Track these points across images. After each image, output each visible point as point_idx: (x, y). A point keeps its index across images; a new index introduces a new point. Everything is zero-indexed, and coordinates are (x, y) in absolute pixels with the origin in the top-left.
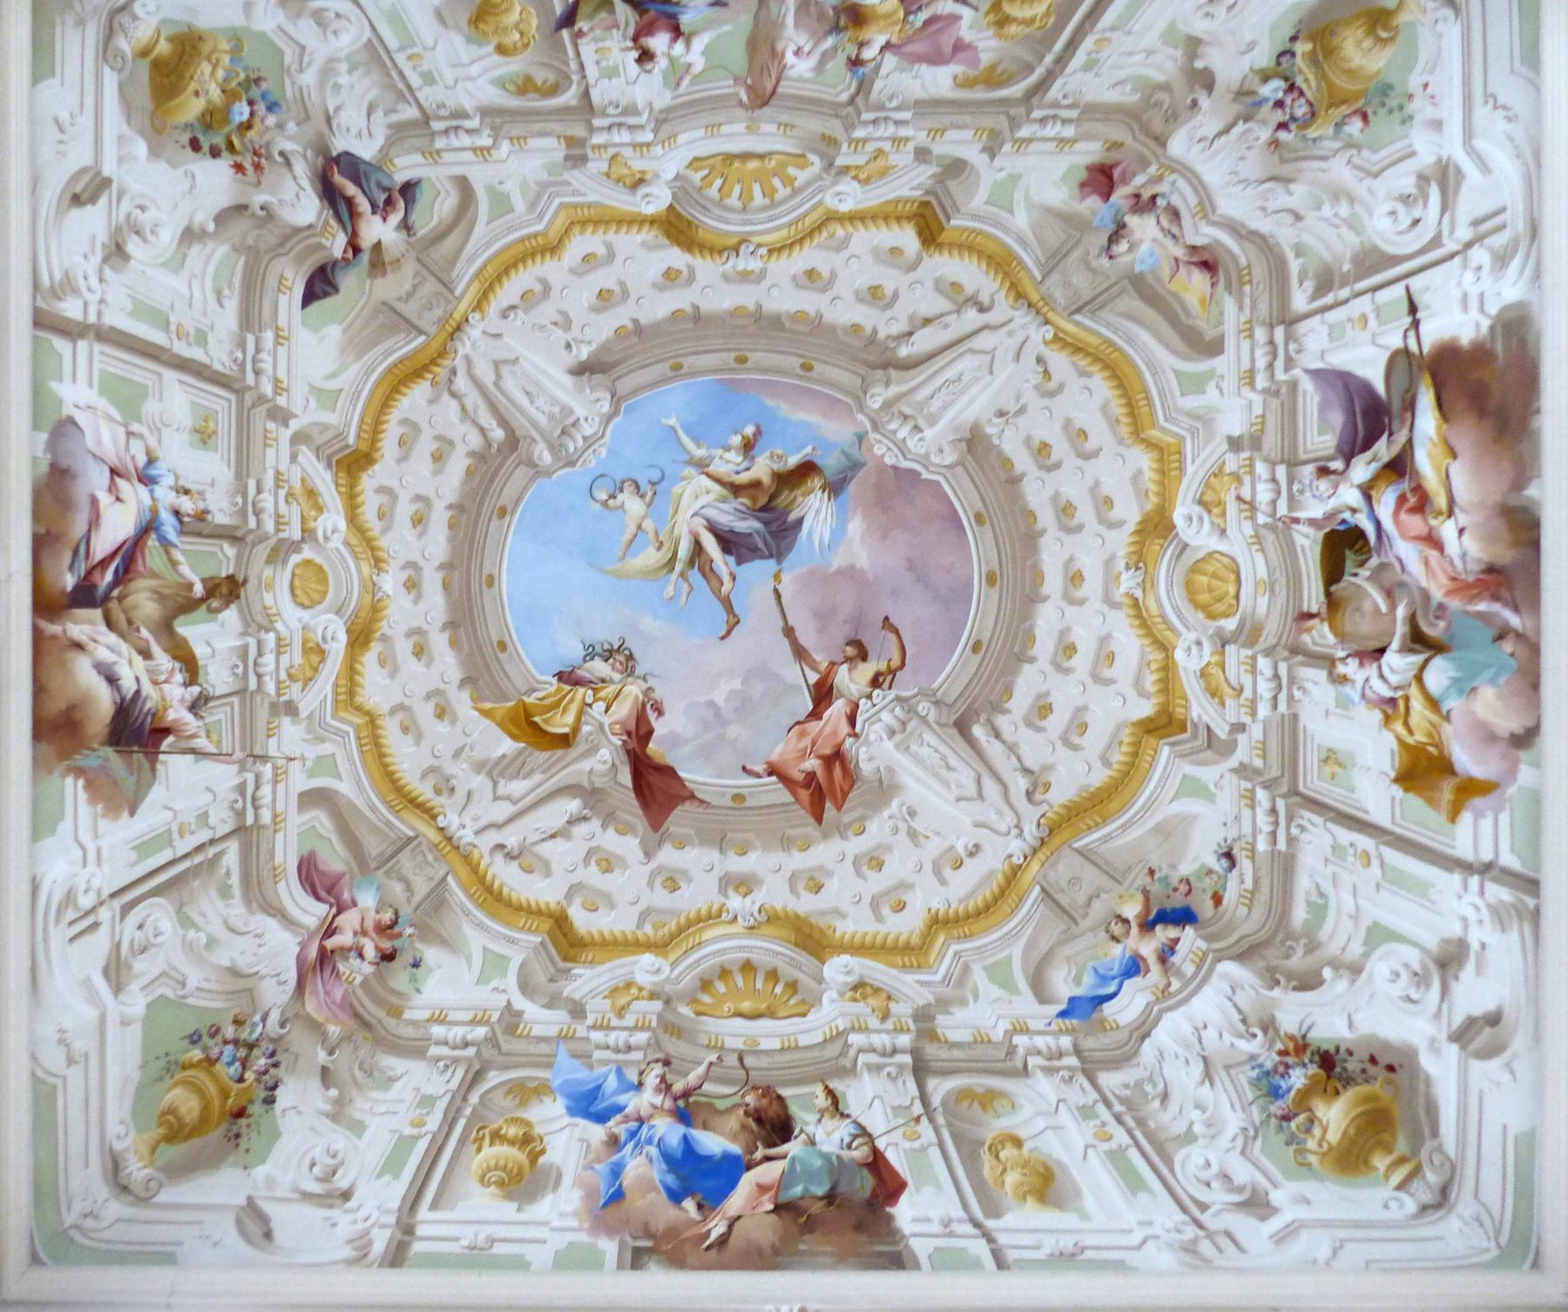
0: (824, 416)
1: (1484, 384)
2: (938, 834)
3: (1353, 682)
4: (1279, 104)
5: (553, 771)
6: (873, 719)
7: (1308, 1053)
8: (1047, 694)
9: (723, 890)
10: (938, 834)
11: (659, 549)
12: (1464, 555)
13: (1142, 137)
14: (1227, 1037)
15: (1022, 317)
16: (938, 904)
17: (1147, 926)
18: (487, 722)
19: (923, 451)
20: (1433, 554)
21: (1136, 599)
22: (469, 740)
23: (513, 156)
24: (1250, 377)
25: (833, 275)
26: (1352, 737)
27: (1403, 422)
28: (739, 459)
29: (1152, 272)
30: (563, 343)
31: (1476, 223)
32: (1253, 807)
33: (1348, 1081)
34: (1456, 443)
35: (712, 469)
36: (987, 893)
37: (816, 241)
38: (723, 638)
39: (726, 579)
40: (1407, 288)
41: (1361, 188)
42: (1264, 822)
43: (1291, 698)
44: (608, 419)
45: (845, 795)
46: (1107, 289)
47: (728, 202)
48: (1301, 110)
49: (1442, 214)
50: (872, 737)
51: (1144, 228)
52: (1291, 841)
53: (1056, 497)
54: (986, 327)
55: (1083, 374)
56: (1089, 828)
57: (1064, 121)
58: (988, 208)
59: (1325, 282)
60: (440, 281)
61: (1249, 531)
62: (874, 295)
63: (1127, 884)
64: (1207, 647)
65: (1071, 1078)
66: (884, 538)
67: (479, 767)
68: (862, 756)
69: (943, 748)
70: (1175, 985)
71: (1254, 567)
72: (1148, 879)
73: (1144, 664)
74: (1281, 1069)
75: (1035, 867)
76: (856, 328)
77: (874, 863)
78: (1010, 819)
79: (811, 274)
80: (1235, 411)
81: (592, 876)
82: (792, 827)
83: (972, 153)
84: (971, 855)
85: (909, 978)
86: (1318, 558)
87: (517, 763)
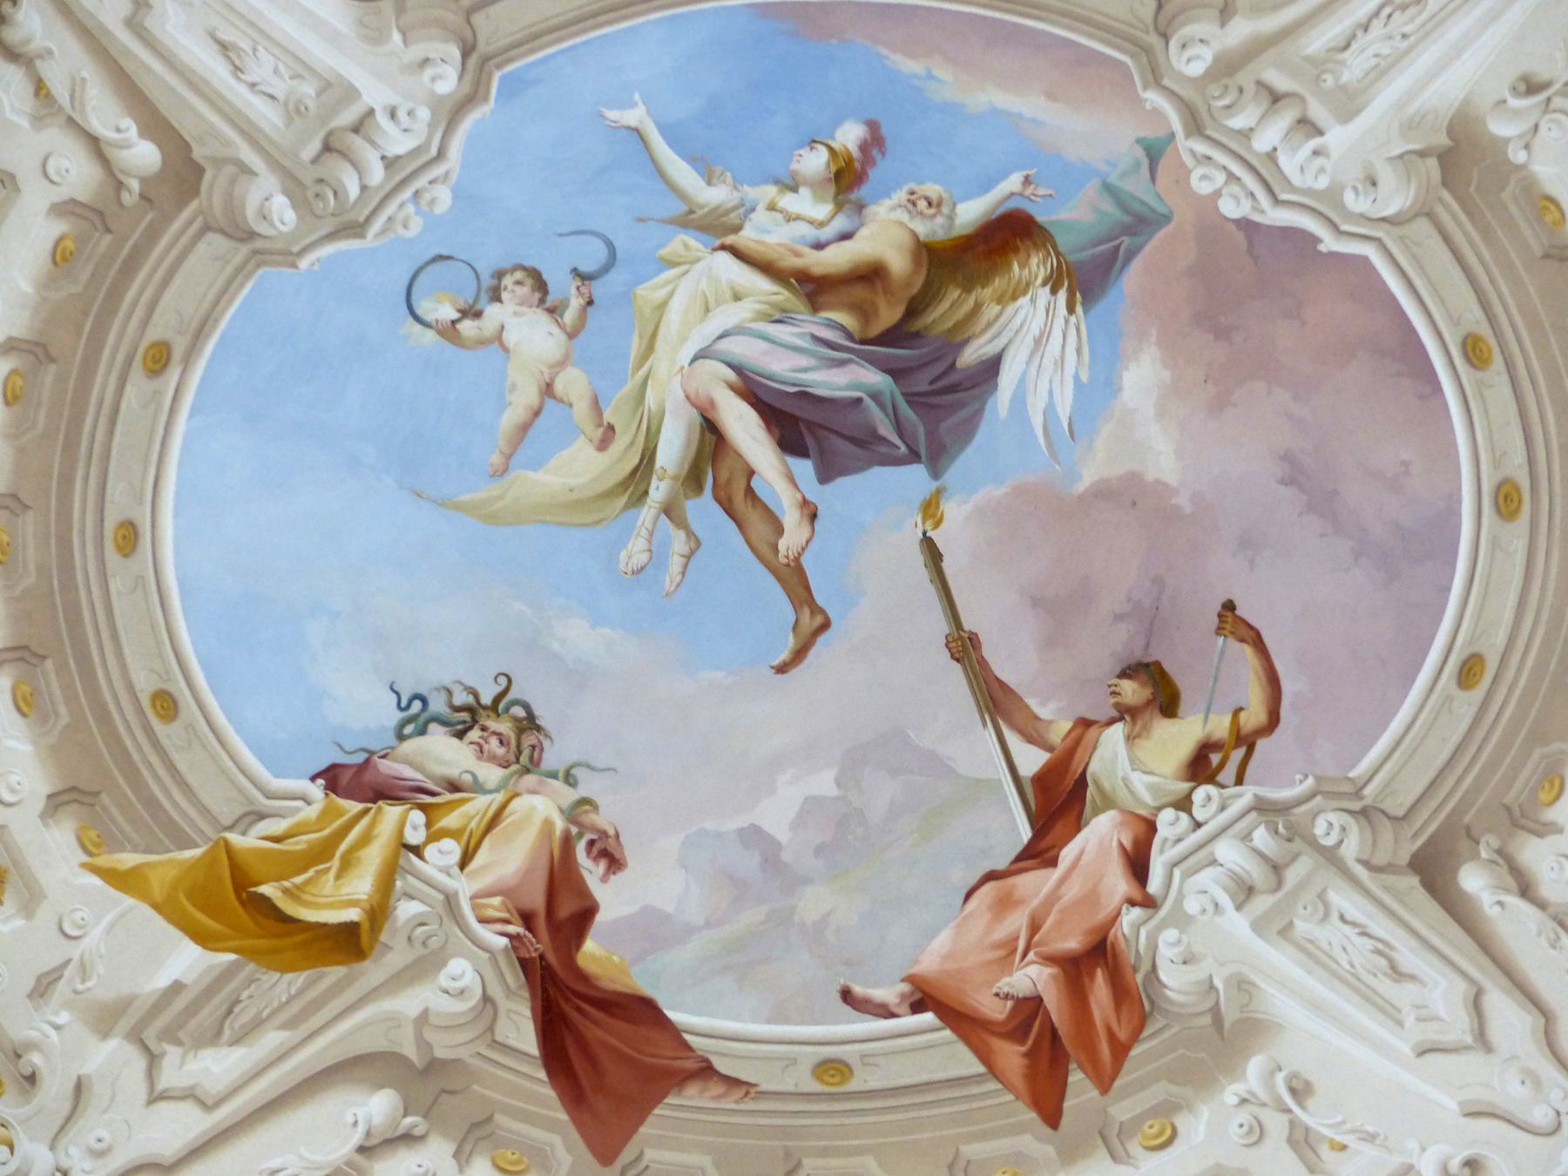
0: (1051, 96)
2: (1371, 1138)
6: (1198, 858)
10: (1371, 1138)
11: (603, 444)
18: (129, 901)
19: (1322, 183)
22: (75, 951)
28: (822, 211)
35: (748, 237)
38: (782, 669)
39: (791, 517)
44: (454, 112)
45: (1120, 1051)
50: (1192, 906)
66: (1219, 405)
67: (105, 1019)
68: (1165, 952)
69: (1381, 927)
82: (984, 1136)
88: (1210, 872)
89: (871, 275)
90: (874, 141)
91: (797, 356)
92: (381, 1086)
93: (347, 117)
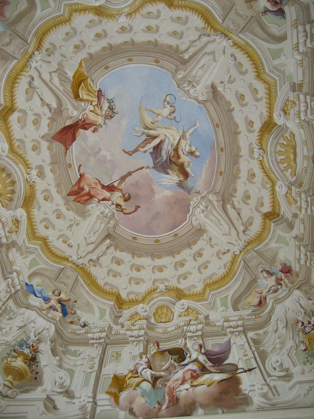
0: (205, 180)
1: (229, 394)
3: (141, 360)
4: (309, 323)
5: (64, 93)
6: (106, 207)
7: (34, 353)
8: (123, 263)
9: (37, 167)
12: (180, 391)
13: (300, 283)
14: (33, 330)
15: (242, 244)
16: (50, 239)
17: (60, 301)
18: (78, 66)
19: (196, 214)
20: (180, 382)
21: (157, 290)
23: (295, 60)
24: (227, 320)
25: (254, 183)
26: (126, 360)
27: (217, 370)
28: (187, 150)
29: (258, 285)
30: (223, 80)
31: (275, 387)
32: (100, 332)
33: (29, 366)
34: (212, 386)
36: (58, 253)
37: (265, 177)
40: (256, 368)
41: (285, 351)
42: (97, 335)
43: (133, 341)
44: (196, 99)
45: (79, 202)
46: (252, 271)
47: (278, 146)
48: (307, 329)
49: (277, 377)
50: (99, 207)
51: (271, 281)
52: (93, 344)
53: (185, 260)
54: (238, 233)
55: (225, 266)
56: (85, 281)
57: (306, 261)
58: (278, 235)
59: (257, 342)
60: (244, 27)
61: (181, 324)
62: (247, 197)
63: (71, 294)
64: (145, 314)
65: (8, 292)
67: (60, 64)
68: (93, 205)
70: (45, 312)
71: (171, 327)
72: (73, 301)
73: (137, 294)
74: (28, 346)
75: (70, 265)
76: (236, 191)
77: (59, 216)
78: (82, 255)
79: (254, 175)
80: (216, 316)
81: (31, 118)
82: (64, 186)
83: (295, 232)
84: (69, 245)
85: (25, 236)
86: (174, 347)
87: (65, 79)
88: (104, 208)
89: (179, 157)
90: (197, 157)
91: (167, 149)
92: (57, 105)
93: (194, 84)
